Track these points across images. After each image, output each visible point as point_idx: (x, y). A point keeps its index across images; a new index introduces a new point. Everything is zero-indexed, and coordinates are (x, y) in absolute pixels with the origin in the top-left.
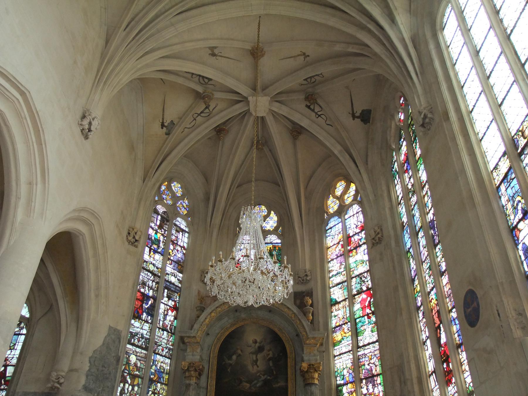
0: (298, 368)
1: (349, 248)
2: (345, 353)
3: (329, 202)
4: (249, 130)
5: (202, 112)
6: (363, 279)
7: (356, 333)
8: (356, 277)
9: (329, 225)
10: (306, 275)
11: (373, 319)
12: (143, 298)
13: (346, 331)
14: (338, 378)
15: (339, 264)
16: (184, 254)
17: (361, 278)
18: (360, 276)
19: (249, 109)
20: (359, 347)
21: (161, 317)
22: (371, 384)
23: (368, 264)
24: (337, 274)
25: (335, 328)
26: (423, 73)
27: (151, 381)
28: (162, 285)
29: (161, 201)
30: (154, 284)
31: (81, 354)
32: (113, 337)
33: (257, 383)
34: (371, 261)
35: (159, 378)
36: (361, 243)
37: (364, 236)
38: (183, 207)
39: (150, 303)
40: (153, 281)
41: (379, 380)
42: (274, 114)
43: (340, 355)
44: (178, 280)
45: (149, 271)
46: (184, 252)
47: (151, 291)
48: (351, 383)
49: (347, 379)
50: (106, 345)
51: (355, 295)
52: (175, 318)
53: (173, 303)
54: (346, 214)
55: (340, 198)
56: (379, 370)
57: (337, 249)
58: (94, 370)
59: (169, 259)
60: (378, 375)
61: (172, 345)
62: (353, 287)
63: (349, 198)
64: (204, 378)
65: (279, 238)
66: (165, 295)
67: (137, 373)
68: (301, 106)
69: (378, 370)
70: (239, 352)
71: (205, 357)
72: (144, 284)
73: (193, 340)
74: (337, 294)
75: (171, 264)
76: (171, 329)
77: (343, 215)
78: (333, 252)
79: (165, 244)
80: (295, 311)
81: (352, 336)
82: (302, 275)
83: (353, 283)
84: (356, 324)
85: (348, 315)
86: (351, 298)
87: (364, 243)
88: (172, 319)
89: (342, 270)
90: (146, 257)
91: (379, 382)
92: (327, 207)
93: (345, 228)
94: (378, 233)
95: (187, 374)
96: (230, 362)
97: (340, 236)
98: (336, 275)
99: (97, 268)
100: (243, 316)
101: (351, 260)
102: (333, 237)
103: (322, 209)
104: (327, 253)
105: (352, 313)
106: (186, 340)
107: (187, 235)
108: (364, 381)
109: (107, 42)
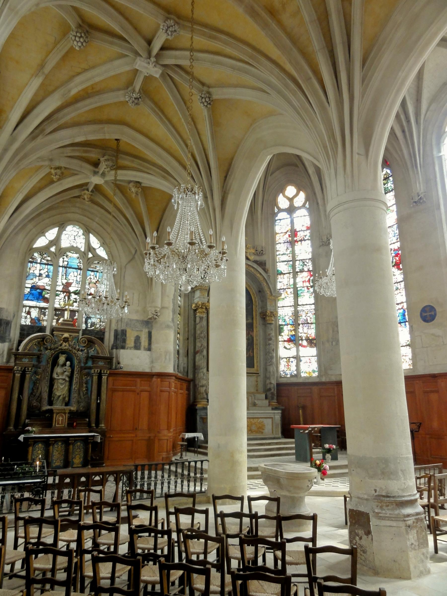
1: (295, 239)
6: (305, 263)
7: (296, 295)
8: (299, 260)
10: (262, 250)
11: (311, 290)
17: (304, 262)
18: (303, 261)
22: (306, 328)
23: (311, 254)
24: (284, 254)
25: (279, 289)
37: (309, 234)
41: (313, 326)
48: (291, 325)
49: (288, 322)
51: (298, 272)
55: (291, 200)
56: (313, 320)
60: (312, 323)
69: (312, 321)
74: (282, 267)
78: (281, 238)
82: (259, 249)
84: (297, 291)
87: (308, 239)
89: (288, 252)
93: (292, 223)
97: (289, 228)
98: (282, 255)
103: (275, 203)
108: (301, 325)
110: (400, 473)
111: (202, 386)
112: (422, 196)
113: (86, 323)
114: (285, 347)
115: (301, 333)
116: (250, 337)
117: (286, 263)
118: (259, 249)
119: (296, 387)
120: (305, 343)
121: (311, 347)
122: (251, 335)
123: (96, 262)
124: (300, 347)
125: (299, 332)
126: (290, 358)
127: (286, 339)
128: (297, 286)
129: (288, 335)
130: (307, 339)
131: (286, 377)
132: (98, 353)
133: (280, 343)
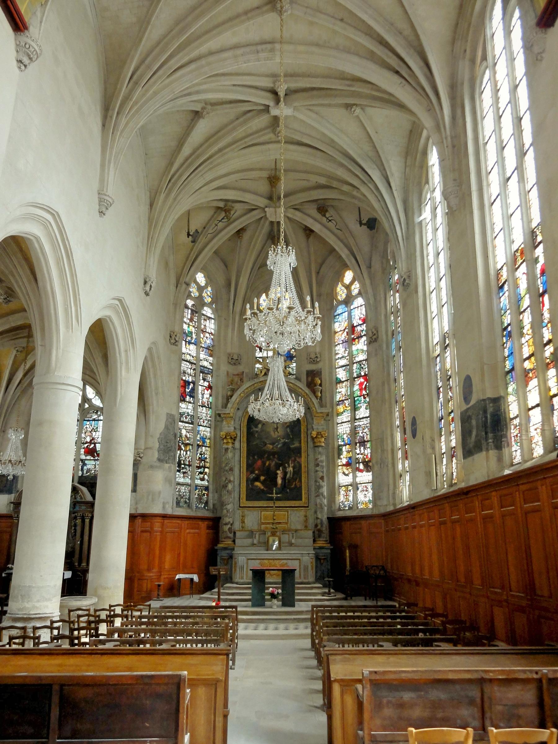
0: (309, 432)
1: (353, 336)
4: (266, 229)
5: (222, 219)
6: (362, 366)
7: (355, 408)
9: (337, 311)
10: (317, 357)
11: (368, 399)
12: (185, 384)
13: (347, 405)
14: (340, 440)
15: (344, 349)
16: (212, 339)
17: (361, 365)
19: (266, 215)
21: (200, 396)
25: (338, 402)
26: (407, 238)
27: (199, 446)
28: (198, 370)
29: (189, 296)
30: (192, 370)
31: (152, 436)
32: (170, 420)
33: (277, 445)
34: (369, 353)
35: (204, 442)
36: (362, 335)
38: (208, 295)
39: (190, 387)
40: (191, 369)
43: (342, 423)
44: (210, 363)
45: (187, 361)
46: (212, 337)
47: (190, 377)
48: (348, 444)
50: (167, 427)
52: (211, 396)
53: (208, 384)
54: (352, 304)
55: (348, 287)
57: (343, 336)
58: (162, 447)
59: (201, 347)
60: (368, 441)
61: (210, 417)
62: (354, 371)
63: (355, 292)
64: (237, 444)
66: (201, 378)
67: (188, 442)
68: (314, 212)
71: (238, 427)
72: (184, 372)
73: (228, 415)
74: (342, 374)
75: (203, 351)
76: (208, 405)
77: (349, 305)
79: (197, 335)
80: (307, 392)
82: (313, 356)
83: (354, 368)
84: (355, 401)
85: (349, 393)
86: (352, 380)
87: (365, 335)
88: (208, 396)
89: (346, 355)
90: (184, 350)
91: (368, 446)
92: (336, 293)
93: (350, 317)
94: (375, 334)
95: (225, 441)
96: (257, 429)
97: (346, 324)
98: (341, 358)
99: (155, 375)
101: (354, 348)
102: (340, 325)
103: (332, 295)
105: (352, 393)
106: (222, 416)
108: (358, 444)
109: (151, 205)
110: (20, 597)
111: (226, 524)
112: (405, 276)
113: (82, 470)
114: (344, 473)
115: (358, 454)
116: (297, 464)
117: (344, 368)
118: (313, 356)
119: (348, 523)
120: (361, 467)
123: (91, 412)
124: (357, 472)
126: (348, 485)
127: (344, 463)
128: (355, 395)
131: (344, 510)
132: (81, 498)
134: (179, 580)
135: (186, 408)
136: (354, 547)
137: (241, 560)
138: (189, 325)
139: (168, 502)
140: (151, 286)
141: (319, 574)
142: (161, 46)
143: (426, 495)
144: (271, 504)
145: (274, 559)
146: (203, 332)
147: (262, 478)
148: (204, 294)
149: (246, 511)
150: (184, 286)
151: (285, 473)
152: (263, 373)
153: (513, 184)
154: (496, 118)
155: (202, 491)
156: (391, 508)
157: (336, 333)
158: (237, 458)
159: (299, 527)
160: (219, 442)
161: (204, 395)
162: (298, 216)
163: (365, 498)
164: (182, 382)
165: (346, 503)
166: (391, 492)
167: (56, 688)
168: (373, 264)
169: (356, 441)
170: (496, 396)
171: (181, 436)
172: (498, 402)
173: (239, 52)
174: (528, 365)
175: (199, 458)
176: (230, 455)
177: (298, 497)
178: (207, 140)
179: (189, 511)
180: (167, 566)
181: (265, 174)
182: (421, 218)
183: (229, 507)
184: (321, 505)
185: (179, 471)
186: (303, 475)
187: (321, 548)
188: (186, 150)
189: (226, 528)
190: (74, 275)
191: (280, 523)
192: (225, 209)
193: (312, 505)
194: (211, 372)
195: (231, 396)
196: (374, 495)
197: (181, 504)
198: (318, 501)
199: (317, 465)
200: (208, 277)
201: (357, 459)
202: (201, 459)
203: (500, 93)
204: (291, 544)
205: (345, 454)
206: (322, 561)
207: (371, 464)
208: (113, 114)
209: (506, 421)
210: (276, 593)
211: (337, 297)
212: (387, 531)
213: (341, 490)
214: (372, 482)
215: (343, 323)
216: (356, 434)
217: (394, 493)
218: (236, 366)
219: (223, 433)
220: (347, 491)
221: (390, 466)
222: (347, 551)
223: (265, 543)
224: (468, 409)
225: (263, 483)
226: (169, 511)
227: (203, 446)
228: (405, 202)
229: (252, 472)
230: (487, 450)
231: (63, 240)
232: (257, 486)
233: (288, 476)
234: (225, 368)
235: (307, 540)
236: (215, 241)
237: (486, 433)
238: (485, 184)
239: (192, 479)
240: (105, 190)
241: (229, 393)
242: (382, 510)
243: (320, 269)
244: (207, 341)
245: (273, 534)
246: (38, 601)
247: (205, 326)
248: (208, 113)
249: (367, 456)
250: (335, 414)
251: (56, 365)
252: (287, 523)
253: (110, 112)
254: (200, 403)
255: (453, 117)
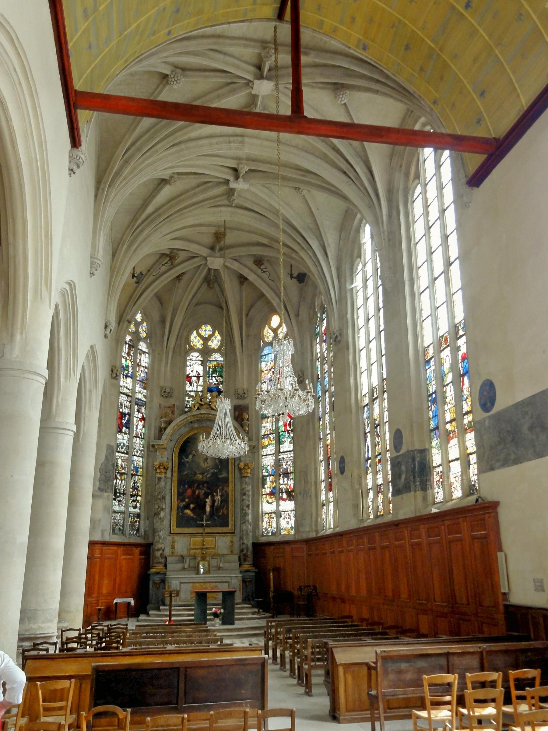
2: (270, 455)
3: (265, 332)
7: (279, 442)
10: (244, 393)
11: (292, 435)
13: (272, 439)
14: (264, 471)
19: (206, 263)
20: (280, 452)
21: (135, 427)
25: (264, 435)
26: (340, 300)
27: (133, 475)
30: (128, 402)
33: (207, 475)
35: (137, 471)
38: (143, 330)
41: (292, 476)
42: (227, 267)
43: (266, 455)
45: (123, 394)
46: (146, 370)
50: (107, 458)
52: (144, 427)
53: (141, 415)
55: (275, 331)
57: (269, 375)
58: (103, 477)
60: (291, 473)
61: (143, 447)
65: (222, 356)
66: (136, 410)
67: (123, 471)
68: (250, 263)
70: (194, 452)
72: (121, 405)
73: (161, 447)
76: (141, 436)
81: (275, 444)
82: (240, 392)
84: (279, 436)
85: (274, 428)
88: (141, 427)
90: (122, 383)
100: (196, 425)
103: (260, 336)
104: (261, 376)
105: (277, 428)
107: (147, 355)
108: (282, 476)
109: (114, 256)
110: (26, 619)
111: (158, 550)
112: (337, 334)
114: (268, 502)
115: (282, 485)
118: (240, 392)
120: (285, 496)
121: (290, 500)
122: (226, 491)
124: (281, 501)
125: (280, 483)
126: (271, 513)
127: (268, 492)
129: (270, 488)
130: (287, 492)
131: (267, 536)
133: (264, 496)
134: (116, 603)
135: (123, 439)
136: (277, 570)
137: (174, 584)
138: (126, 359)
139: (106, 530)
140: (111, 330)
141: (244, 596)
142: (151, 132)
143: (352, 524)
144: (200, 530)
145: (205, 583)
146: (139, 366)
147: (192, 506)
148: (140, 330)
149: (177, 538)
150: (126, 323)
151: (213, 501)
152: (196, 408)
153: (440, 283)
154: (427, 228)
155: (134, 518)
156: (313, 535)
157: (262, 371)
158: (168, 487)
159: (226, 553)
160: (151, 472)
161: (139, 427)
162: (235, 266)
163: (287, 524)
164: (119, 414)
165: (269, 529)
166: (314, 520)
167: (182, 670)
168: (300, 313)
169: (278, 471)
170: (422, 448)
171: (117, 466)
172: (425, 453)
173: (214, 140)
174: (449, 427)
175: (133, 487)
176: (162, 484)
177: (225, 524)
178: (170, 201)
179: (123, 537)
180: (104, 591)
181: (213, 230)
182: (353, 286)
183: (161, 533)
184: (247, 532)
185: (115, 499)
186: (230, 503)
187: (247, 571)
188: (150, 209)
189: (158, 554)
190: (76, 332)
191: (207, 548)
192: (170, 257)
193: (237, 531)
194: (144, 404)
195: (165, 428)
196: (296, 522)
197: (116, 531)
198: (244, 527)
199: (244, 494)
200: (144, 314)
201: (280, 489)
202: (134, 488)
203: (430, 209)
204: (219, 568)
205: (269, 483)
206: (247, 584)
207: (293, 494)
208: (105, 187)
209: (430, 469)
210: (219, 612)
211: (264, 338)
212: (310, 555)
213: (264, 517)
214: (295, 510)
215: (269, 363)
216: (280, 466)
217: (317, 521)
218: (167, 399)
219: (157, 463)
220: (270, 518)
221: (313, 496)
222: (272, 574)
223: (195, 567)
224: (398, 456)
225: (192, 510)
226: (107, 538)
227: (136, 475)
228: (338, 269)
229: (183, 500)
230: (415, 491)
231: (73, 305)
232: (187, 514)
233: (216, 504)
234: (157, 400)
235: (233, 564)
236: (157, 283)
237: (414, 478)
238: (415, 276)
239: (127, 507)
240: (96, 254)
241: (163, 425)
242: (305, 536)
243: (248, 312)
244: (141, 374)
245: (203, 559)
246: (43, 622)
247: (140, 360)
248: (175, 181)
249: (290, 487)
250: (260, 447)
251: (56, 413)
252: (214, 548)
253: (102, 186)
254: (135, 435)
255: (390, 216)
